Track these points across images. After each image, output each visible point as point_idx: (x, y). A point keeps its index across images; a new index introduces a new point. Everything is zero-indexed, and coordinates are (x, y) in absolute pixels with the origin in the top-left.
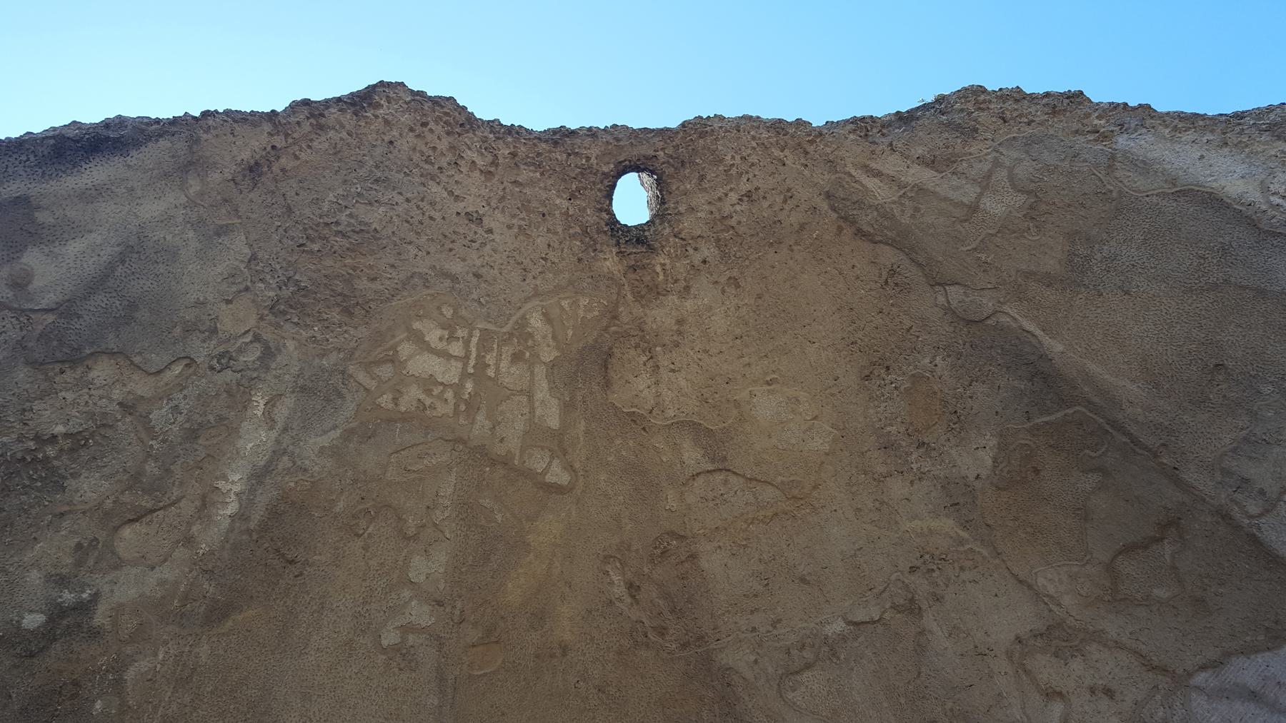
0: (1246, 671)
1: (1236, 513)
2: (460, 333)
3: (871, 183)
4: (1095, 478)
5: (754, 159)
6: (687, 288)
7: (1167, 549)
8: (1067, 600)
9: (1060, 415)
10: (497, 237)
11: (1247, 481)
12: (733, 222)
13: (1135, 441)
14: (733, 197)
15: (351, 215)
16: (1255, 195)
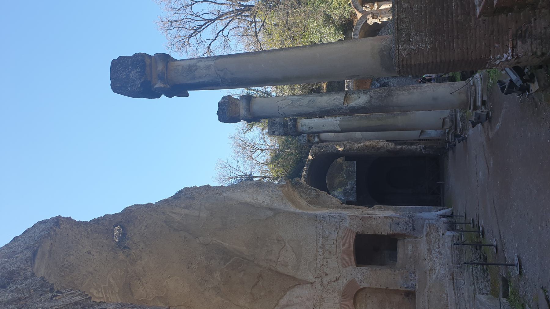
0: (283, 302)
1: (272, 268)
2: (100, 290)
3: (174, 216)
4: (242, 273)
5: (145, 216)
6: (141, 257)
7: (260, 283)
8: (246, 305)
9: (231, 261)
10: (95, 257)
11: (271, 260)
12: (145, 235)
13: (249, 260)
14: (143, 228)
15: (67, 261)
16: (252, 201)
